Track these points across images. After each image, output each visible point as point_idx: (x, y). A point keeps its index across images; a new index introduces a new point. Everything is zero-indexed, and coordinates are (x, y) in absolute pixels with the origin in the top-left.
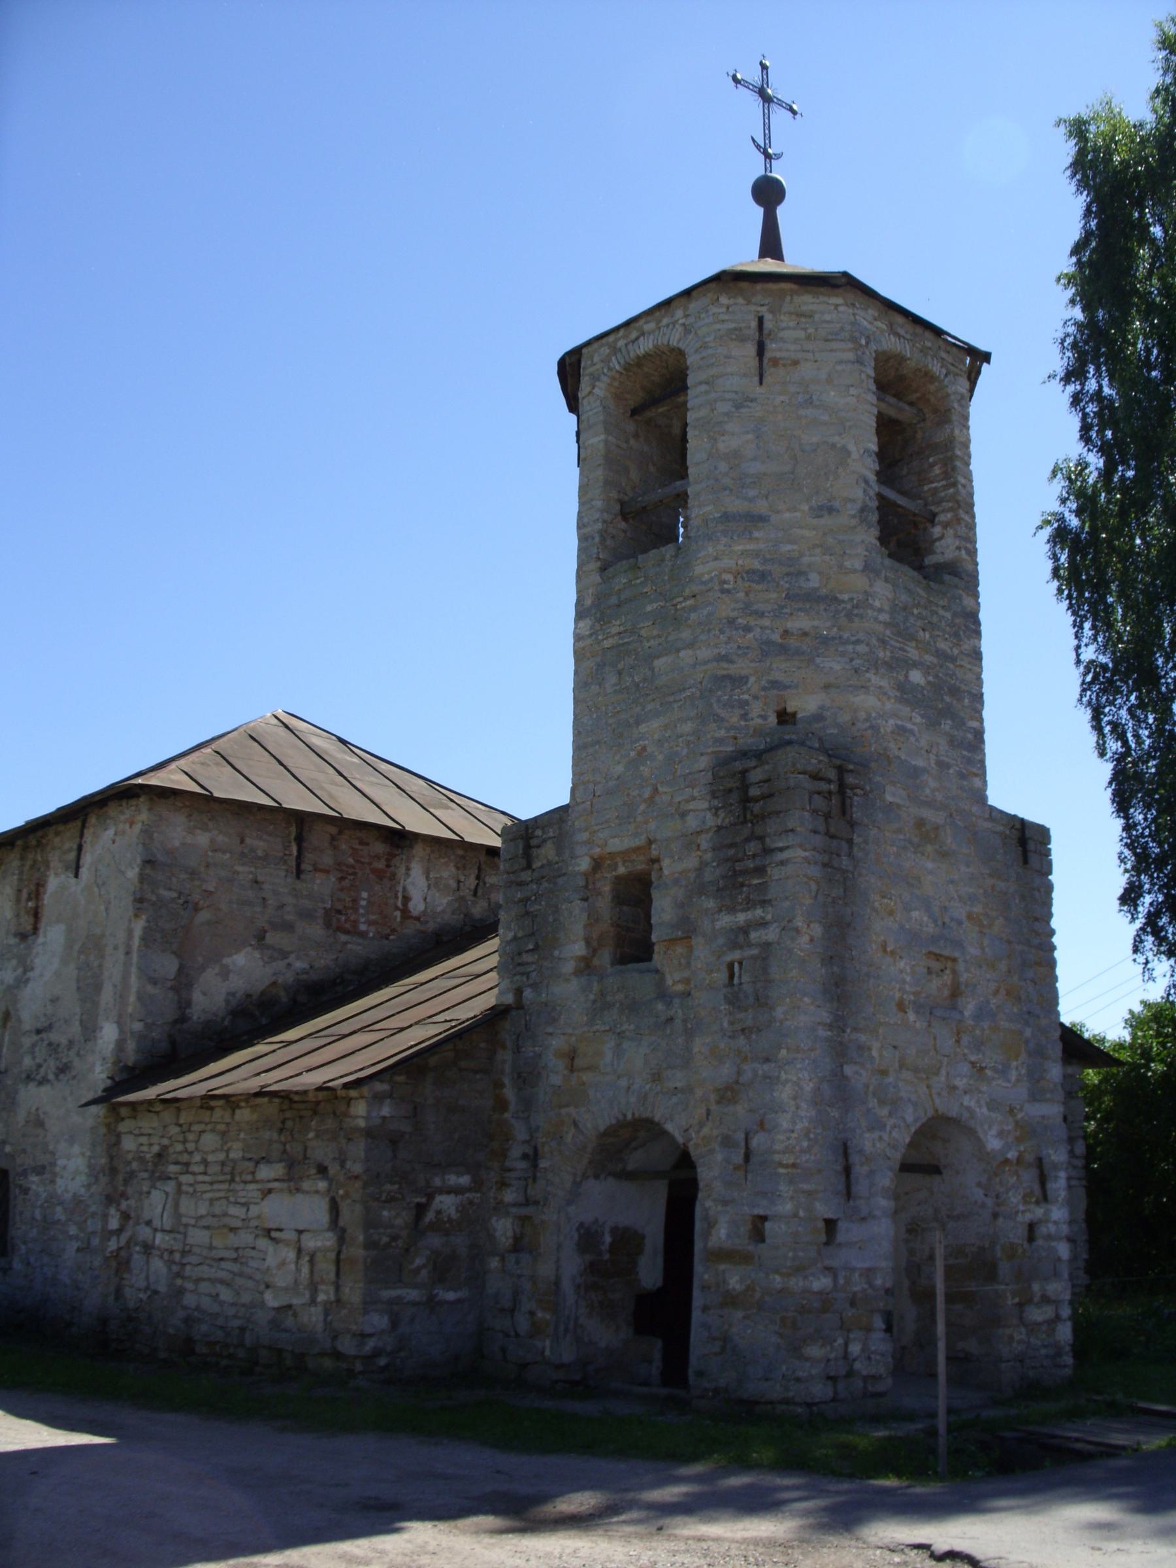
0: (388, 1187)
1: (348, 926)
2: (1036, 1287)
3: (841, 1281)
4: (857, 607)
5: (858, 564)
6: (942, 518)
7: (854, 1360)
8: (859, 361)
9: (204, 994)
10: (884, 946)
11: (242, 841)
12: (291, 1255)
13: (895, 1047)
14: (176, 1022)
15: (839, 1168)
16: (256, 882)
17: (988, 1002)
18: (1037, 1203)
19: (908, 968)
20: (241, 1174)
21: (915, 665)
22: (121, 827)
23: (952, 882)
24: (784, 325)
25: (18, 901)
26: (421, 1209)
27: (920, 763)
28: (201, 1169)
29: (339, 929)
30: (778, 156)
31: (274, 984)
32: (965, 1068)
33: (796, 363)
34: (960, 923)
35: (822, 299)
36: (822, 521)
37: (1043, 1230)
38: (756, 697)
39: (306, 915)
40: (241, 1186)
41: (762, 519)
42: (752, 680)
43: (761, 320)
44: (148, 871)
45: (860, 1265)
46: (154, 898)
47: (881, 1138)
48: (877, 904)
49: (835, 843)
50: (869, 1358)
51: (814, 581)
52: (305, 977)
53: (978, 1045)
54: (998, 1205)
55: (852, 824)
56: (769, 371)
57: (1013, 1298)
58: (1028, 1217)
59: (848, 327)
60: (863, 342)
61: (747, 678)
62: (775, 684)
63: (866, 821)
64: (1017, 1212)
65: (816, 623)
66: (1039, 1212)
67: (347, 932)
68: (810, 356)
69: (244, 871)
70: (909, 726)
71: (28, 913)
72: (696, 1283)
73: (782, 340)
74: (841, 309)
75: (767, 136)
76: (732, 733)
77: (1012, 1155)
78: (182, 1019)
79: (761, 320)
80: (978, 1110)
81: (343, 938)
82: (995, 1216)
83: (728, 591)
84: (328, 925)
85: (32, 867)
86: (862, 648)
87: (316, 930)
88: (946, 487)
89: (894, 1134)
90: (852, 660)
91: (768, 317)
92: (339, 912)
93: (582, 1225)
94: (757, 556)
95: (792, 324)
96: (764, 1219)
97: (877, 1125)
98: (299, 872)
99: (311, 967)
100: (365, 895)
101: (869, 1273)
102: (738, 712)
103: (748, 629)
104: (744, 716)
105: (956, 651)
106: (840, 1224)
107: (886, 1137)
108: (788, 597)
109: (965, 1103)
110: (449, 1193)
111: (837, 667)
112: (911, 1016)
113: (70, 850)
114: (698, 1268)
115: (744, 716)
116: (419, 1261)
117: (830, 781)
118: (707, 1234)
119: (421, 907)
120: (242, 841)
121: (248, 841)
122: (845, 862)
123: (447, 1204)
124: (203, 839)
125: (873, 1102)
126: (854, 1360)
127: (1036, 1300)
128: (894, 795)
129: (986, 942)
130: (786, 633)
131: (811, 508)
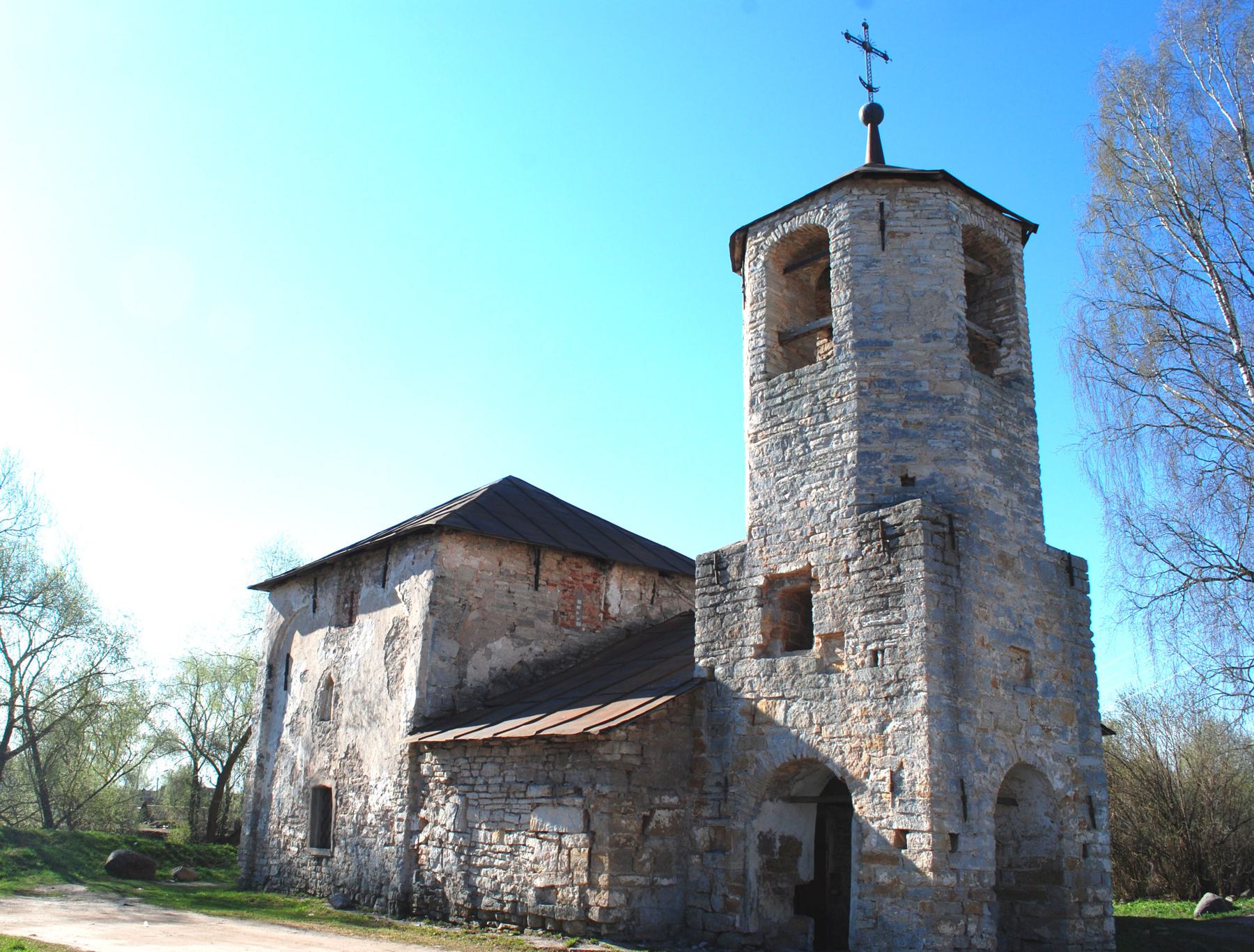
0: (625, 803)
1: (568, 623)
2: (1090, 891)
3: (962, 879)
4: (956, 404)
5: (956, 375)
6: (1007, 341)
7: (972, 937)
8: (952, 233)
9: (475, 668)
10: (982, 641)
11: (500, 564)
12: (554, 851)
13: (991, 713)
14: (456, 687)
16: (509, 592)
18: (1088, 829)
20: (514, 793)
21: (995, 444)
22: (418, 553)
23: (1024, 597)
24: (898, 208)
25: (338, 603)
26: (646, 820)
27: (1001, 513)
28: (485, 788)
29: (564, 625)
30: (877, 90)
31: (521, 662)
32: (1038, 730)
33: (907, 235)
34: (1031, 626)
35: (924, 189)
36: (929, 345)
38: (886, 467)
39: (541, 615)
40: (515, 801)
41: (888, 344)
42: (883, 455)
43: (882, 205)
44: (439, 584)
45: (974, 868)
46: (443, 602)
47: (985, 777)
48: (976, 611)
49: (948, 568)
50: (982, 937)
51: (925, 387)
52: (540, 657)
54: (1062, 829)
55: (959, 556)
56: (889, 240)
57: (1075, 898)
58: (1083, 839)
59: (944, 209)
60: (954, 219)
61: (879, 454)
62: (899, 458)
63: (968, 553)
64: (1075, 835)
65: (927, 416)
66: (1090, 835)
67: (568, 627)
68: (917, 229)
69: (503, 584)
70: (994, 488)
71: (344, 611)
72: (853, 877)
73: (897, 219)
74: (939, 196)
75: (870, 76)
76: (870, 492)
77: (1070, 793)
78: (461, 685)
79: (882, 205)
81: (566, 631)
82: (1060, 837)
83: (865, 394)
84: (555, 622)
85: (348, 580)
86: (960, 433)
87: (547, 626)
88: (1009, 320)
89: (993, 775)
90: (953, 441)
91: (887, 203)
92: (563, 613)
93: (761, 833)
94: (885, 369)
95: (903, 207)
96: (905, 832)
97: (982, 768)
98: (536, 586)
99: (545, 651)
100: (579, 602)
101: (980, 875)
102: (874, 477)
103: (879, 420)
104: (879, 480)
105: (1021, 435)
107: (988, 776)
108: (907, 398)
110: (664, 809)
111: (943, 446)
112: (1002, 692)
113: (378, 569)
114: (855, 866)
115: (879, 480)
116: (644, 856)
117: (943, 525)
118: (861, 842)
119: (617, 611)
120: (500, 564)
121: (504, 564)
122: (955, 582)
123: (662, 816)
124: (474, 562)
125: (979, 752)
126: (972, 937)
127: (1090, 900)
128: (985, 536)
130: (906, 423)
131: (921, 336)
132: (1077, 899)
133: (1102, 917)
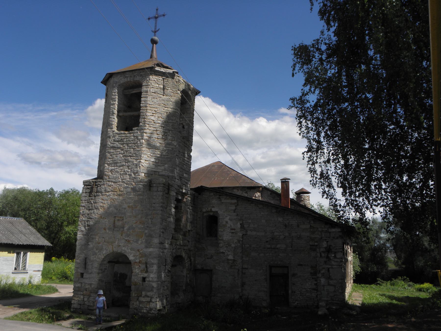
2: (144, 293)
3: (83, 285)
7: (85, 301)
15: (84, 263)
17: (132, 225)
19: (107, 221)
34: (125, 209)
37: (147, 279)
50: (89, 302)
53: (128, 236)
57: (135, 294)
58: (142, 276)
64: (139, 274)
77: (137, 261)
80: (127, 250)
97: (95, 254)
101: (91, 284)
106: (84, 274)
107: (97, 257)
109: (123, 249)
112: (108, 231)
126: (85, 301)
129: (134, 212)
132: (136, 295)
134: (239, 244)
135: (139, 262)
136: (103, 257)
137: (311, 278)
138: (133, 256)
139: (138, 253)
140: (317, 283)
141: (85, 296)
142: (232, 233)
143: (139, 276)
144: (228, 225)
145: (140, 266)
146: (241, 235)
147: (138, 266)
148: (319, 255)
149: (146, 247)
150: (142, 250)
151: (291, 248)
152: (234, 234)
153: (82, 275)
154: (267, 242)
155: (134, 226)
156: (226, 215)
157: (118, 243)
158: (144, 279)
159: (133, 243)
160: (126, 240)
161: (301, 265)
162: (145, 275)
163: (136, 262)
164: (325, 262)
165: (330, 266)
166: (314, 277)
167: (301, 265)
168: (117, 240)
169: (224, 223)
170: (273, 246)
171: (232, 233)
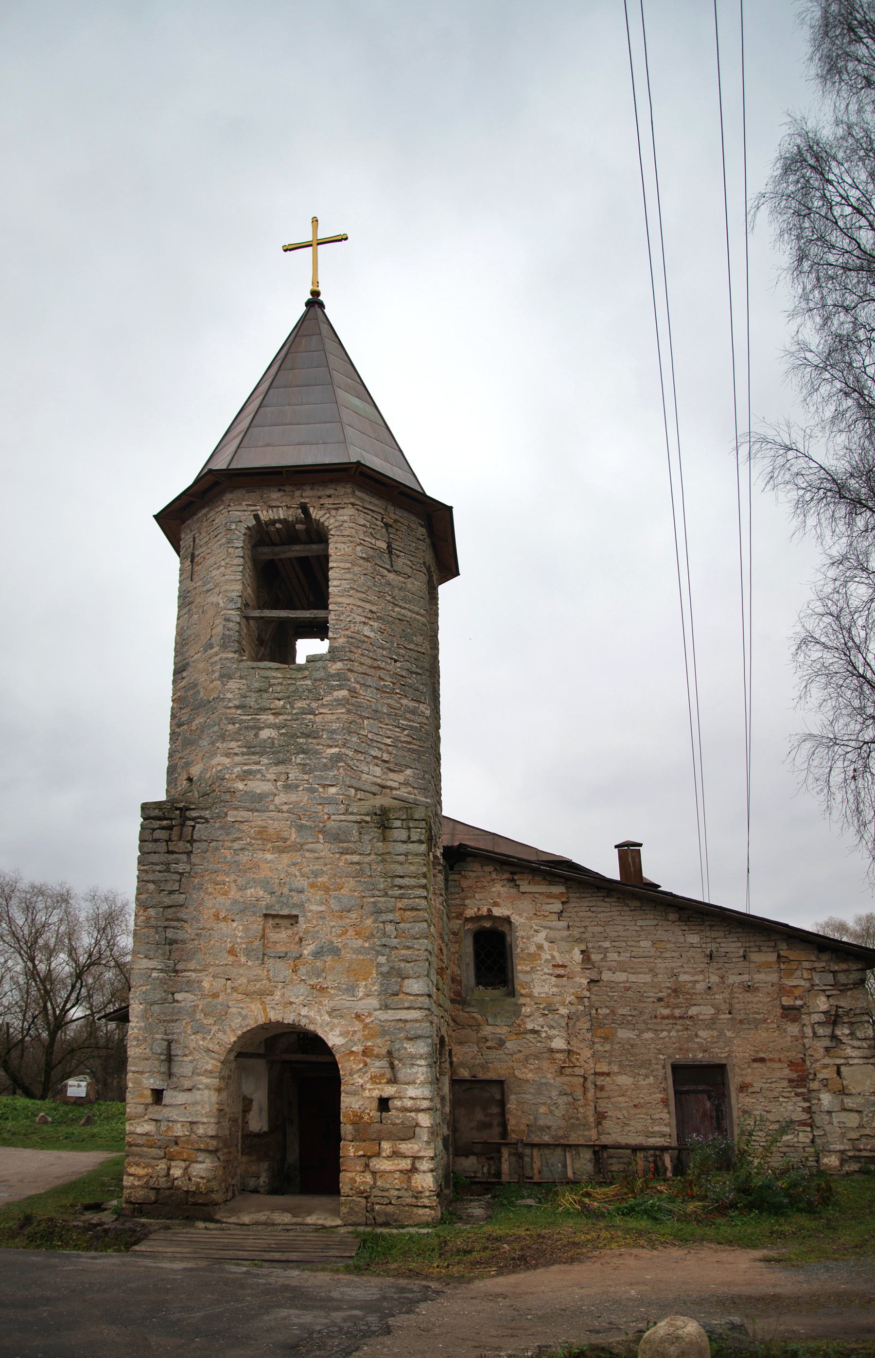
10: (217, 917)
19: (241, 928)
23: (294, 864)
32: (303, 989)
50: (190, 1179)
58: (376, 1093)
70: (255, 767)
80: (318, 1018)
106: (165, 1092)
112: (243, 960)
127: (384, 1154)
133: (410, 1171)
134: (581, 1008)
135: (364, 1053)
136: (233, 1039)
137: (793, 1094)
138: (341, 1035)
139: (358, 1026)
140: (809, 1107)
141: (173, 1163)
142: (559, 976)
143: (367, 1093)
144: (546, 956)
145: (366, 1065)
146: (585, 982)
147: (361, 1065)
148: (808, 1031)
149: (386, 1007)
150: (370, 1015)
151: (729, 1016)
152: (565, 979)
153: (158, 1095)
154: (660, 1000)
155: (338, 942)
156: (536, 928)
157: (283, 995)
158: (384, 1104)
159: (338, 996)
160: (313, 987)
161: (762, 1060)
162: (389, 1091)
163: (352, 1052)
164: (827, 1049)
165: (842, 1061)
166: (799, 1090)
167: (762, 1060)
168: (280, 985)
169: (533, 949)
170: (677, 1012)
171: (559, 976)
